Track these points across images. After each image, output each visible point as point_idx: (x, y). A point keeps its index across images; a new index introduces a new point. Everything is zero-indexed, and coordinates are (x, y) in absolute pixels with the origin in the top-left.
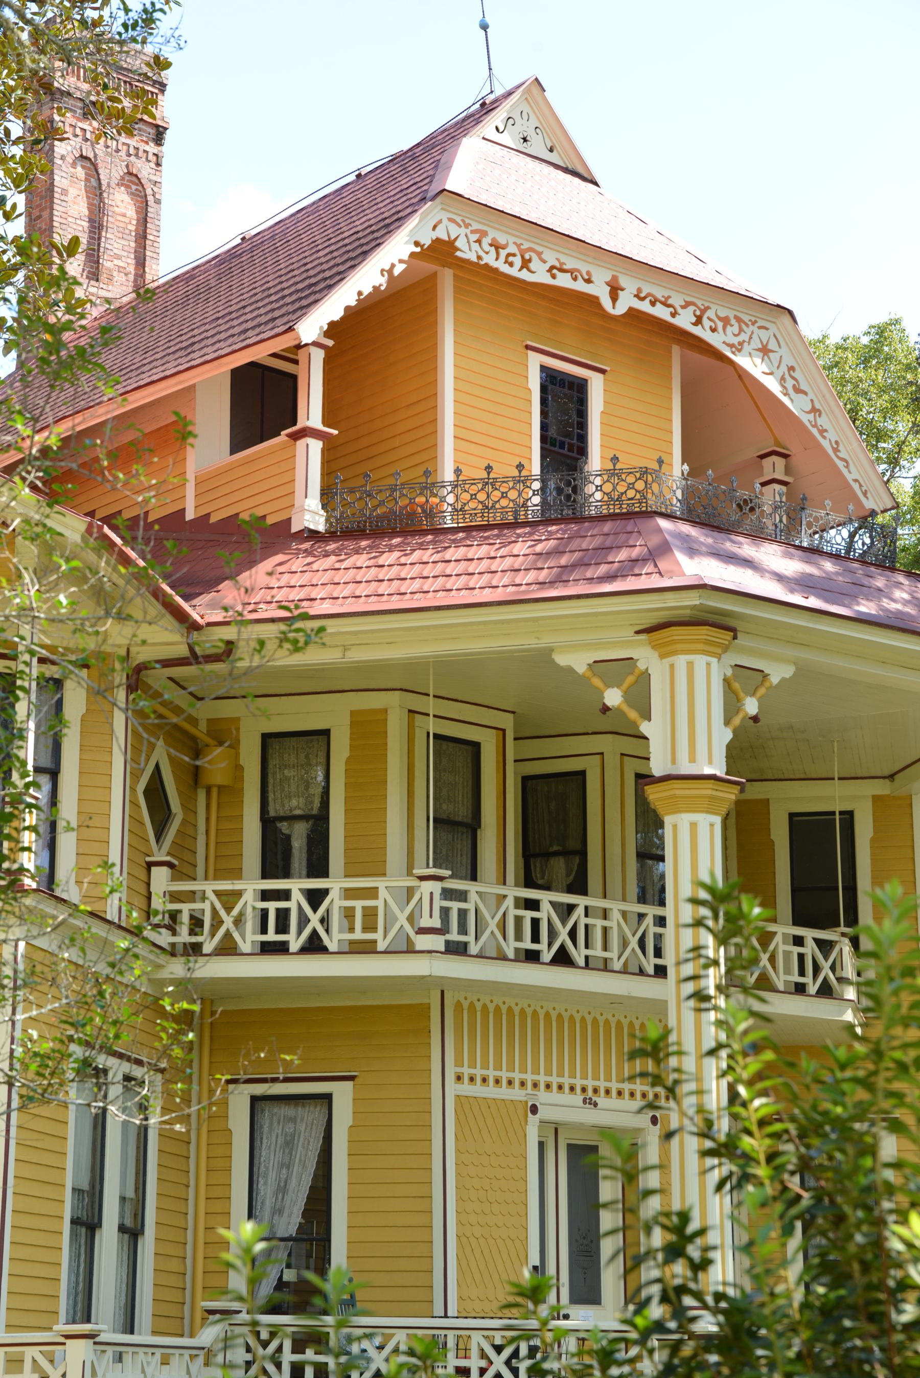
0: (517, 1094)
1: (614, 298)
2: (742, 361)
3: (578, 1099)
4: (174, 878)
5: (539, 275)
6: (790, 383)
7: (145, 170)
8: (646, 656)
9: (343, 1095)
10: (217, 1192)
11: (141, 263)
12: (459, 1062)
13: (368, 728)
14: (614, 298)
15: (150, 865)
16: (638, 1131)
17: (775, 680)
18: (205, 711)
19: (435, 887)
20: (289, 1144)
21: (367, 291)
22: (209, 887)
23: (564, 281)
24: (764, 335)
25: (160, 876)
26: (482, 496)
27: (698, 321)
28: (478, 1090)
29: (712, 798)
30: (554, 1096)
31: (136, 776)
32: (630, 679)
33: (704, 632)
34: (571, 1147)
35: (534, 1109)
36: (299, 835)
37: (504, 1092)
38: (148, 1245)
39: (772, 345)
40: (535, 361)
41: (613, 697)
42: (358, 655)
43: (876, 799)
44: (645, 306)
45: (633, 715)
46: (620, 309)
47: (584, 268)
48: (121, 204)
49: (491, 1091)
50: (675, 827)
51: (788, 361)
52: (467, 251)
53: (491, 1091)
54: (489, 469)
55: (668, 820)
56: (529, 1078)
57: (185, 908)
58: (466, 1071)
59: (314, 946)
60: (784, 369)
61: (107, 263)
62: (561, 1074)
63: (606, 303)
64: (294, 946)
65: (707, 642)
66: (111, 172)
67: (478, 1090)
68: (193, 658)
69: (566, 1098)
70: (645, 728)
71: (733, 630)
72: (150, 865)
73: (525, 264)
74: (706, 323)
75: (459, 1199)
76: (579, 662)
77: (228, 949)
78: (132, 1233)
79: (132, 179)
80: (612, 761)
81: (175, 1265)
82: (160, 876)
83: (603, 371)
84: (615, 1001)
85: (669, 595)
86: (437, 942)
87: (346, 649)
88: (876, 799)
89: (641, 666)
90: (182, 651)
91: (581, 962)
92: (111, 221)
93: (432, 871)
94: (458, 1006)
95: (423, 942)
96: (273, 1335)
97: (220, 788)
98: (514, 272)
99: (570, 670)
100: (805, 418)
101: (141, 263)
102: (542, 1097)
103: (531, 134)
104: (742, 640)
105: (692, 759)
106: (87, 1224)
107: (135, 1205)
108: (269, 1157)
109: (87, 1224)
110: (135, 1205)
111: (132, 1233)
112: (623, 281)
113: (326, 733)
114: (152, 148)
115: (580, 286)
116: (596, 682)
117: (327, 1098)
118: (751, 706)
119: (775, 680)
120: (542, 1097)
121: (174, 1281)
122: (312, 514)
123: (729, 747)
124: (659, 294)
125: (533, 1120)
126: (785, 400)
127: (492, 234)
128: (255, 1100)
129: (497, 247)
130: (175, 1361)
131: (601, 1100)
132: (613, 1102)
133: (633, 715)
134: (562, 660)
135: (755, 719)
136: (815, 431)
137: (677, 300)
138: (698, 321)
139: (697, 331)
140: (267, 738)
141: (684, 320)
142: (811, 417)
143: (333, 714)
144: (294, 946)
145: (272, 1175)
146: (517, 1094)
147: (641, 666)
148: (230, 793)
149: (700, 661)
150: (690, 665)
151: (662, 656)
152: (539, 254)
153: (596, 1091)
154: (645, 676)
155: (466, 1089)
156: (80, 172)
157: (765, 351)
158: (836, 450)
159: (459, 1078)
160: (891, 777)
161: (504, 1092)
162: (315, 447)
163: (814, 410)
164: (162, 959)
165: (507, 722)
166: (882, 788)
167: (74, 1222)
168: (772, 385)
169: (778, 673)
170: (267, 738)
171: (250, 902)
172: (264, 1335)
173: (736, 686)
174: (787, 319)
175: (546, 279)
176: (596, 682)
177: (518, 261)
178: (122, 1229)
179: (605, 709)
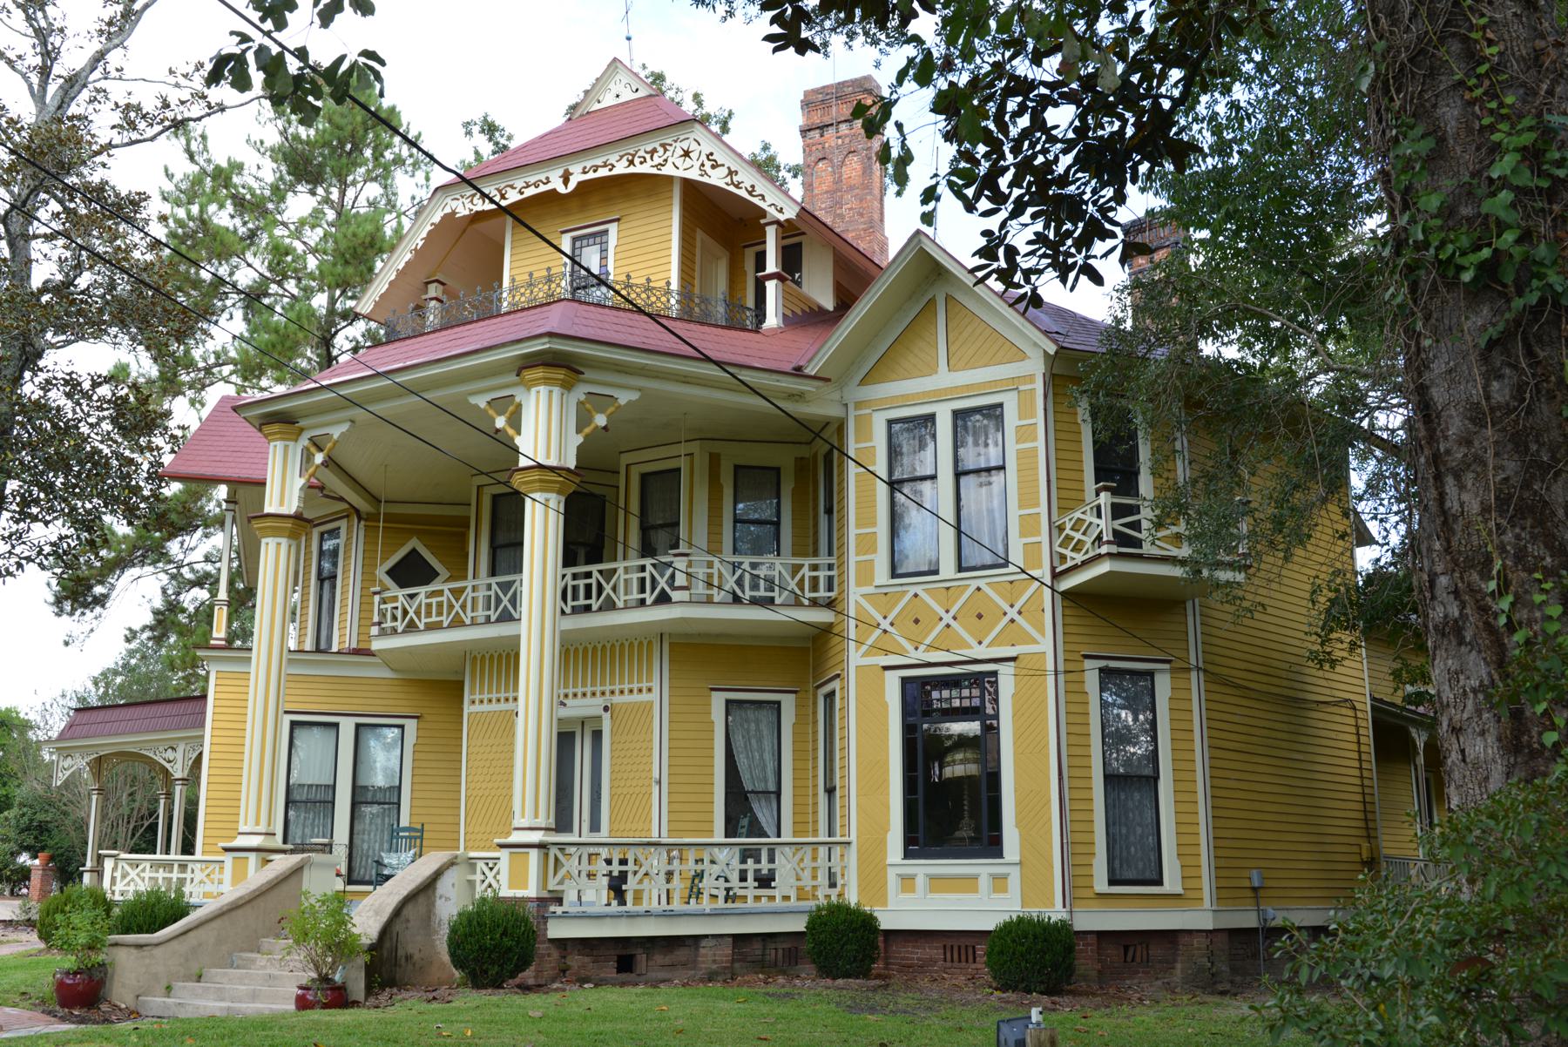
5: (513, 197)
6: (708, 164)
12: (472, 692)
27: (631, 163)
28: (486, 707)
39: (694, 146)
44: (591, 175)
46: (572, 185)
52: (463, 211)
58: (477, 697)
60: (703, 157)
62: (584, 685)
63: (562, 190)
74: (637, 161)
83: (618, 220)
91: (468, 621)
100: (721, 184)
115: (543, 188)
123: (579, 448)
124: (599, 162)
126: (705, 179)
132: (580, 701)
136: (732, 189)
137: (613, 159)
138: (631, 163)
139: (632, 170)
141: (621, 168)
142: (728, 180)
152: (512, 187)
153: (566, 696)
155: (477, 708)
158: (750, 193)
163: (731, 173)
169: (336, 432)
175: (520, 197)
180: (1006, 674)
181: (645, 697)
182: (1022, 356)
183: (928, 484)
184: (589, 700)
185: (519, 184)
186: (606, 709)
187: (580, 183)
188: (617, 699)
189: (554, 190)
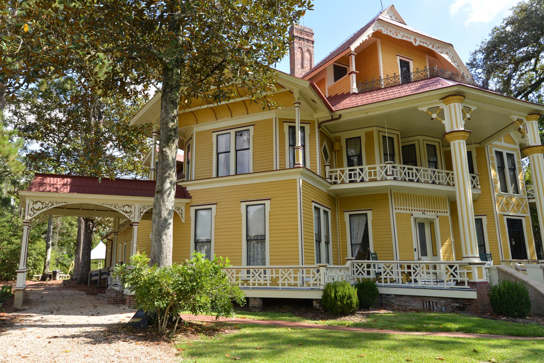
0: (408, 212)
1: (415, 42)
2: (443, 55)
3: (421, 212)
4: (330, 168)
5: (399, 37)
7: (311, 49)
8: (442, 106)
9: (370, 214)
10: (343, 235)
11: (311, 65)
12: (395, 205)
13: (369, 136)
14: (415, 42)
15: (325, 166)
16: (434, 219)
17: (473, 110)
18: (333, 135)
19: (390, 165)
20: (358, 224)
21: (364, 40)
22: (338, 170)
23: (405, 39)
24: (447, 50)
25: (327, 168)
26: (394, 80)
27: (433, 47)
28: (400, 211)
29: (464, 136)
30: (416, 212)
31: (321, 147)
32: (438, 111)
33: (458, 97)
34: (419, 223)
35: (412, 215)
36: (355, 159)
37: (405, 212)
38: (330, 245)
40: (398, 58)
41: (434, 116)
42: (369, 114)
43: (476, 148)
45: (440, 119)
46: (417, 45)
47: (409, 36)
48: (307, 55)
49: (402, 211)
50: (454, 144)
51: (452, 56)
52: (384, 32)
53: (402, 211)
54: (395, 74)
55: (452, 143)
56: (411, 208)
57: (333, 174)
58: (397, 207)
59: (362, 181)
61: (305, 65)
63: (414, 43)
64: (358, 181)
65: (459, 100)
66: (305, 49)
67: (400, 211)
68: (333, 119)
69: (419, 212)
70: (443, 122)
71: (465, 96)
72: (325, 166)
73: (397, 35)
75: (398, 235)
76: (425, 109)
77: (343, 182)
78: (327, 243)
79: (308, 50)
80: (421, 141)
81: (336, 250)
82: (327, 168)
84: (429, 190)
85: (449, 88)
86: (392, 178)
87: (367, 113)
88: (476, 148)
89: (441, 108)
90: (330, 118)
92: (305, 58)
93: (389, 162)
94: (394, 193)
95: (388, 178)
96: (362, 265)
97: (338, 151)
98: (394, 36)
99: (422, 111)
101: (311, 65)
102: (414, 212)
103: (392, 16)
104: (466, 100)
105: (457, 127)
106: (319, 241)
107: (327, 237)
108: (355, 227)
109: (319, 241)
110: (327, 237)
111: (327, 243)
112: (417, 39)
113: (360, 137)
114: (312, 45)
115: (408, 40)
116: (430, 113)
117: (366, 214)
118: (468, 116)
119: (473, 110)
120: (414, 212)
121: (336, 253)
122: (354, 88)
124: (425, 41)
125: (412, 217)
126: (452, 64)
127: (389, 29)
128: (350, 215)
129: (390, 30)
130: (342, 271)
131: (426, 213)
132: (428, 213)
133: (440, 119)
134: (420, 109)
135: (469, 119)
138: (433, 47)
139: (433, 49)
140: (347, 140)
141: (430, 47)
143: (361, 133)
144: (358, 181)
145: (355, 231)
146: (408, 212)
147: (441, 108)
148: (340, 151)
149: (457, 104)
150: (454, 105)
151: (446, 105)
154: (443, 110)
155: (397, 211)
156: (299, 50)
157: (447, 53)
159: (396, 209)
160: (480, 143)
161: (405, 212)
162: (354, 76)
164: (329, 185)
165: (399, 133)
166: (478, 146)
167: (316, 241)
168: (449, 60)
169: (473, 108)
170: (347, 140)
171: (347, 172)
172: (360, 265)
173: (464, 111)
174: (451, 47)
176: (430, 113)
177: (395, 34)
178: (325, 242)
179: (432, 119)
180: (523, 219)
181: (446, 214)
182: (515, 144)
183: (247, 151)
184: (431, 213)
185: (402, 34)
186: (437, 217)
187: (419, 45)
188: (439, 214)
189: (411, 43)
